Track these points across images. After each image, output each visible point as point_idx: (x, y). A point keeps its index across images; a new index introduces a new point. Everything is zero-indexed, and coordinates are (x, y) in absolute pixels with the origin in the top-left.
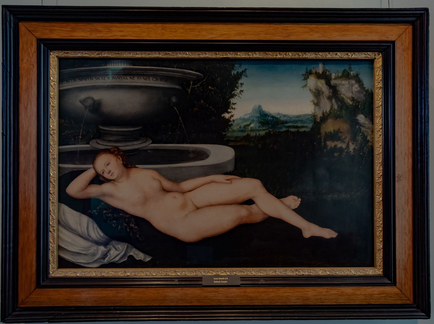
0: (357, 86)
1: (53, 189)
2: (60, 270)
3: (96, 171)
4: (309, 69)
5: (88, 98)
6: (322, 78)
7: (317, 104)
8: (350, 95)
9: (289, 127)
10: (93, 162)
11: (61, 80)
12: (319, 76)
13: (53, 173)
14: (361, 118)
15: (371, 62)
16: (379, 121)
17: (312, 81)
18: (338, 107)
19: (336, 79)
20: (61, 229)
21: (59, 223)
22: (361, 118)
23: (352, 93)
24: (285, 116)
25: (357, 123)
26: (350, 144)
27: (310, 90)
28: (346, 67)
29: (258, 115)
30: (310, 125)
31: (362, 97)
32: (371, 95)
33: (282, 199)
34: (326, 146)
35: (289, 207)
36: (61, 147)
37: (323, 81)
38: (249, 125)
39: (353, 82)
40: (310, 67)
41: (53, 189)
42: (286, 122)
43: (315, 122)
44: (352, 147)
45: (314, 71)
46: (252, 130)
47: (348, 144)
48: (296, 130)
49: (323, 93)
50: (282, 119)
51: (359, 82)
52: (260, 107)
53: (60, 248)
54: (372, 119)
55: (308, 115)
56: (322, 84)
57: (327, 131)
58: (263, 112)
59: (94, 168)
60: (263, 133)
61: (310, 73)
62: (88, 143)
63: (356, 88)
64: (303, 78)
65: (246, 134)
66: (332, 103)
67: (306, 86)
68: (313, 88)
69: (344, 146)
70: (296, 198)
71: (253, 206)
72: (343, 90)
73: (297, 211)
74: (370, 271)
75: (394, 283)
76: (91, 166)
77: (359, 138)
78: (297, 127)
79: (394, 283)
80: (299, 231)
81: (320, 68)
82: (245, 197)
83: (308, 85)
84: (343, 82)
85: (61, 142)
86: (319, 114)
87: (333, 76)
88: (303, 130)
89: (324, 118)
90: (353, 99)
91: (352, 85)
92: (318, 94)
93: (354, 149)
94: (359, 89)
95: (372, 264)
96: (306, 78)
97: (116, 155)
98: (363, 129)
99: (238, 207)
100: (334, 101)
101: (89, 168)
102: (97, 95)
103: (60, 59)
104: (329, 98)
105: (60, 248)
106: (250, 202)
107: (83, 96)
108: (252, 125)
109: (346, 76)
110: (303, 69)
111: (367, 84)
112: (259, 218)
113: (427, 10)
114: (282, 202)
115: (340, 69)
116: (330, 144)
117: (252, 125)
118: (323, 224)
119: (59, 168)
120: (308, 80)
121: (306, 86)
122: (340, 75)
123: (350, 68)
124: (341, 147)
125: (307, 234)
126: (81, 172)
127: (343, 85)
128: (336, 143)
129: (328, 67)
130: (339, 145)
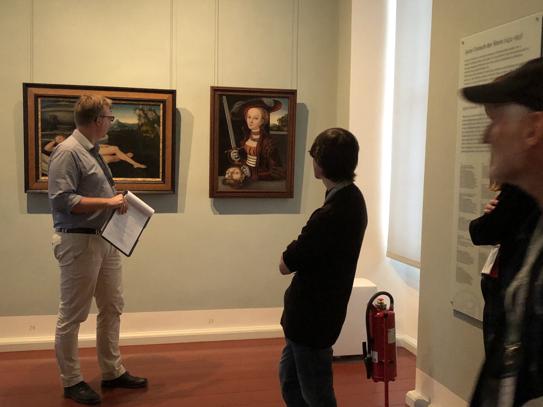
0: (154, 114)
1: (40, 148)
2: (43, 177)
3: (56, 142)
4: (136, 107)
5: (52, 115)
6: (141, 110)
7: (139, 120)
8: (152, 117)
9: (129, 128)
10: (54, 138)
11: (42, 108)
12: (140, 110)
13: (40, 142)
14: (156, 126)
15: (160, 105)
16: (161, 127)
17: (138, 112)
18: (147, 121)
19: (146, 111)
20: (42, 162)
21: (42, 160)
22: (156, 126)
23: (153, 116)
24: (128, 124)
25: (155, 127)
26: (152, 135)
27: (137, 115)
28: (150, 107)
29: (117, 123)
30: (137, 128)
31: (156, 118)
32: (159, 117)
33: (127, 154)
34: (143, 135)
35: (129, 157)
36: (42, 133)
37: (142, 112)
38: (114, 126)
39: (153, 112)
40: (137, 106)
41: (40, 148)
42: (128, 126)
43: (139, 126)
44: (152, 136)
45: (138, 108)
46: (115, 128)
47: (151, 135)
48: (132, 129)
49: (141, 116)
50: (126, 125)
51: (155, 112)
52: (118, 120)
53: (42, 169)
54: (160, 126)
55: (136, 124)
56: (141, 113)
57: (143, 130)
58: (119, 122)
59: (55, 141)
60: (119, 130)
61: (137, 108)
62: (52, 131)
63: (154, 114)
64: (134, 110)
65: (113, 130)
66: (145, 119)
67: (135, 113)
68: (138, 114)
69: (149, 135)
70: (131, 154)
71: (115, 156)
72: (149, 115)
73: (131, 158)
74: (158, 180)
75: (164, 183)
76: (53, 140)
77: (155, 133)
78: (132, 128)
79: (164, 183)
80: (132, 165)
81: (141, 106)
82: (114, 153)
83: (136, 113)
84: (149, 112)
85: (42, 131)
86: (140, 124)
87: (146, 110)
88: (134, 129)
89: (142, 125)
90: (153, 118)
91: (153, 113)
92: (139, 116)
93: (153, 137)
94: (155, 115)
95: (159, 178)
96: (135, 110)
97: (63, 136)
98: (156, 130)
99: (110, 156)
100: (145, 119)
101: (53, 141)
102: (56, 114)
103: (41, 100)
104: (144, 118)
105: (42, 169)
106: (114, 154)
107: (50, 114)
108: (115, 127)
109: (150, 110)
110: (134, 106)
111: (157, 112)
112: (118, 160)
113: (175, 91)
114: (126, 155)
115: (148, 107)
116: (144, 135)
117: (115, 127)
118: (141, 163)
119: (41, 140)
120: (136, 111)
121: (135, 113)
122: (148, 109)
123: (152, 107)
124: (148, 136)
125: (135, 167)
126: (49, 142)
127: (149, 113)
128: (146, 134)
129: (144, 106)
130: (148, 135)
